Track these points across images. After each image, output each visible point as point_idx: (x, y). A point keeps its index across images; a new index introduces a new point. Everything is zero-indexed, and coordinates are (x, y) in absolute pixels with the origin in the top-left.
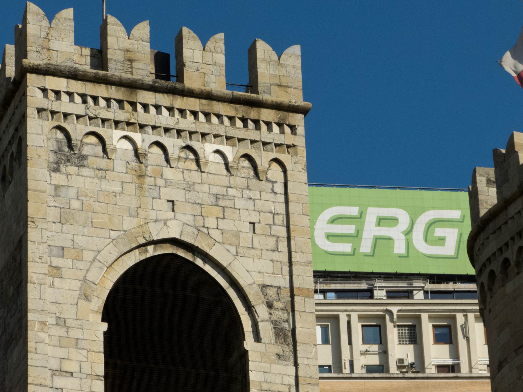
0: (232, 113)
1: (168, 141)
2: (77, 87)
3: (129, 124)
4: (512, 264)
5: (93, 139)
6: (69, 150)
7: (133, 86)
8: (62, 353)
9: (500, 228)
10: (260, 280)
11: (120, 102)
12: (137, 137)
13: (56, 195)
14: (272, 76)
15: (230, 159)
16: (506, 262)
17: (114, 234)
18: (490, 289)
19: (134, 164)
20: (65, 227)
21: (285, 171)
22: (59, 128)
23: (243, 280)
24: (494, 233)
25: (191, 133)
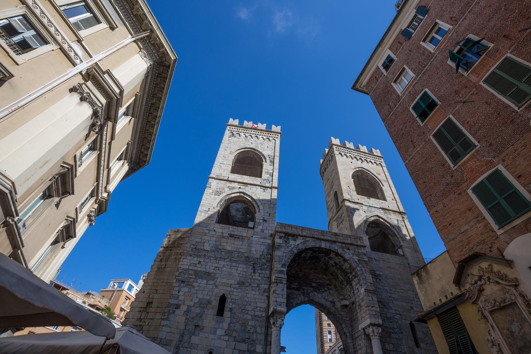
12: (247, 134)
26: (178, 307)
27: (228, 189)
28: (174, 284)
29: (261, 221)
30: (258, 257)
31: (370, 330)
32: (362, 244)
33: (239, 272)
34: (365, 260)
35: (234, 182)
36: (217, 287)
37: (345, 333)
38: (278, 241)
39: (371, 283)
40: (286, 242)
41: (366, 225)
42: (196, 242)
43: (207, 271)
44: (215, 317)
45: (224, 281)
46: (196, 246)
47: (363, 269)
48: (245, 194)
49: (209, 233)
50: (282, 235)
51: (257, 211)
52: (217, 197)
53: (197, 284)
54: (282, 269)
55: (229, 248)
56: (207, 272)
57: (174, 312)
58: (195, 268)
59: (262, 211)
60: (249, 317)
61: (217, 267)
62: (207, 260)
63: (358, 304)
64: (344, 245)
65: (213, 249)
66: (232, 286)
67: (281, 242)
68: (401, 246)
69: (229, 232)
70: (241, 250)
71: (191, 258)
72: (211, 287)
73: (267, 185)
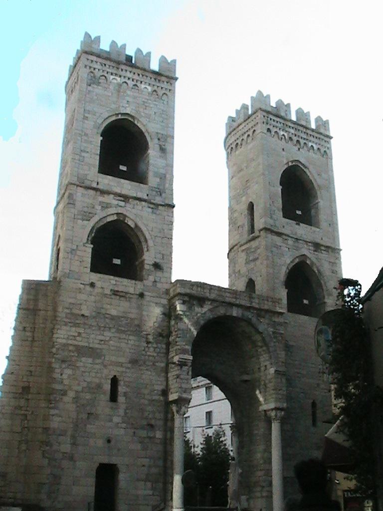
0: (151, 76)
1: (129, 82)
2: (99, 60)
3: (116, 74)
4: (239, 144)
5: (104, 78)
6: (94, 81)
7: (119, 63)
10: (157, 131)
11: (113, 67)
12: (119, 79)
13: (89, 94)
18: (231, 153)
23: (151, 130)
24: (233, 135)
26: (64, 393)
27: (100, 207)
28: (54, 365)
29: (152, 269)
31: (273, 414)
32: (281, 311)
33: (130, 346)
35: (108, 193)
36: (105, 366)
39: (283, 362)
41: (288, 271)
42: (70, 303)
43: (91, 346)
45: (113, 359)
46: (71, 309)
48: (125, 216)
50: (186, 299)
51: (145, 249)
53: (82, 364)
54: (187, 347)
55: (114, 312)
56: (90, 348)
57: (62, 399)
58: (76, 343)
59: (152, 250)
60: (146, 402)
61: (102, 341)
62: (88, 331)
63: (263, 383)
64: (259, 312)
65: (94, 313)
66: (124, 365)
67: (185, 310)
68: (325, 303)
69: (111, 287)
70: (131, 316)
71: (68, 328)
72: (97, 367)
73: (158, 200)
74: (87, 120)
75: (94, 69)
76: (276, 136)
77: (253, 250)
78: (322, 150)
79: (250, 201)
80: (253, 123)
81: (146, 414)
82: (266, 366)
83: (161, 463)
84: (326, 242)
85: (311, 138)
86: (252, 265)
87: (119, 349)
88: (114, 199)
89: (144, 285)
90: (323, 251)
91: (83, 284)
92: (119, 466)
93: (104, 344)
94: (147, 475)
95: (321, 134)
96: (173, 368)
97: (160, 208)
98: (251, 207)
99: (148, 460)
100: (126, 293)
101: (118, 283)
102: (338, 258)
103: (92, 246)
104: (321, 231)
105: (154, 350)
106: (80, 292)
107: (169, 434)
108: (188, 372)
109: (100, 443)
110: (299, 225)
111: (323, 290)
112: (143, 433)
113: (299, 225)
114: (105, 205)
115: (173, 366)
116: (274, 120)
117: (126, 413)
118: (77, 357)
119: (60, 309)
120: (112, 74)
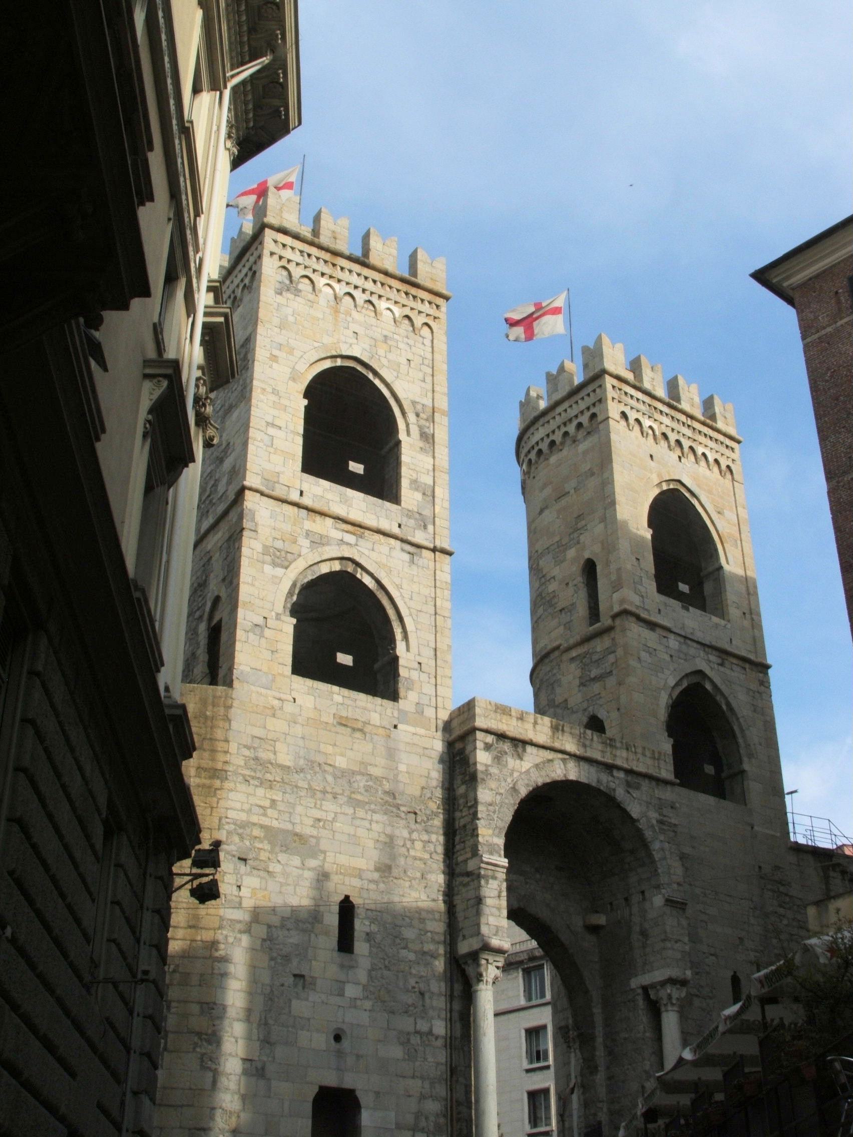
0: (400, 287)
1: (357, 294)
3: (331, 277)
4: (557, 443)
5: (307, 281)
8: (275, 412)
9: (548, 422)
11: (326, 262)
14: (427, 272)
15: (397, 315)
16: (553, 443)
17: (316, 345)
18: (536, 462)
19: (333, 303)
20: (283, 332)
21: (432, 332)
22: (284, 267)
23: (401, 395)
25: (372, 293)
30: (417, 793)
31: (663, 993)
34: (673, 821)
37: (587, 992)
38: (482, 758)
39: (679, 884)
40: (498, 759)
41: (671, 702)
42: (254, 737)
43: (298, 829)
44: (336, 954)
45: (343, 859)
47: (666, 845)
48: (358, 564)
49: (281, 708)
50: (490, 739)
51: (398, 635)
52: (279, 571)
55: (341, 762)
56: (296, 834)
58: (265, 821)
60: (412, 956)
61: (319, 820)
62: (290, 798)
63: (637, 928)
66: (364, 876)
67: (489, 762)
68: (743, 772)
71: (251, 789)
73: (419, 537)
74: (277, 362)
75: (289, 261)
76: (637, 428)
77: (595, 657)
78: (724, 463)
79: (587, 555)
80: (589, 401)
81: (412, 982)
82: (643, 892)
83: (441, 1090)
84: (740, 647)
85: (701, 439)
86: (596, 687)
87: (354, 840)
88: (336, 528)
89: (399, 710)
90: (734, 667)
91: (279, 699)
92: (359, 1094)
93: (324, 827)
94: (418, 1115)
95: (718, 431)
96: (466, 885)
97: (425, 553)
98: (590, 569)
99: (419, 1082)
100: (364, 723)
101: (349, 702)
102: (765, 683)
103: (294, 621)
104: (729, 626)
105: (424, 847)
106: (274, 716)
107: (458, 1026)
108: (499, 896)
109: (321, 1040)
110: (688, 610)
111: (737, 743)
112: (406, 1023)
113: (688, 610)
114: (316, 538)
115: (466, 880)
116: (632, 397)
117: (370, 976)
118: (271, 852)
119: (233, 747)
120: (323, 274)
